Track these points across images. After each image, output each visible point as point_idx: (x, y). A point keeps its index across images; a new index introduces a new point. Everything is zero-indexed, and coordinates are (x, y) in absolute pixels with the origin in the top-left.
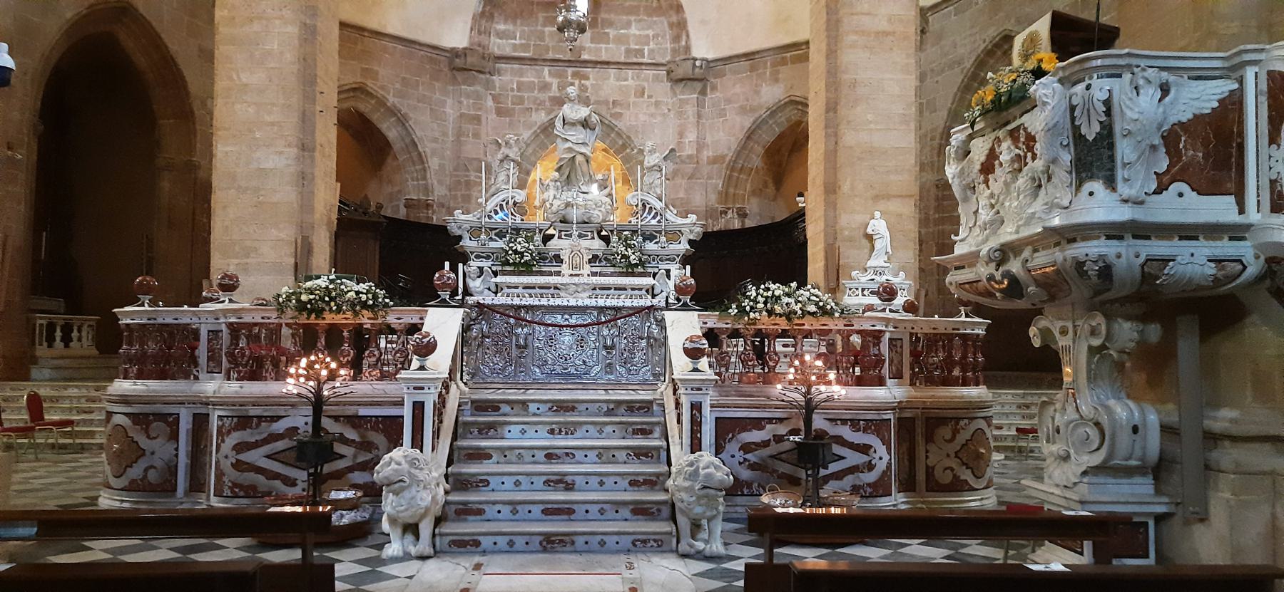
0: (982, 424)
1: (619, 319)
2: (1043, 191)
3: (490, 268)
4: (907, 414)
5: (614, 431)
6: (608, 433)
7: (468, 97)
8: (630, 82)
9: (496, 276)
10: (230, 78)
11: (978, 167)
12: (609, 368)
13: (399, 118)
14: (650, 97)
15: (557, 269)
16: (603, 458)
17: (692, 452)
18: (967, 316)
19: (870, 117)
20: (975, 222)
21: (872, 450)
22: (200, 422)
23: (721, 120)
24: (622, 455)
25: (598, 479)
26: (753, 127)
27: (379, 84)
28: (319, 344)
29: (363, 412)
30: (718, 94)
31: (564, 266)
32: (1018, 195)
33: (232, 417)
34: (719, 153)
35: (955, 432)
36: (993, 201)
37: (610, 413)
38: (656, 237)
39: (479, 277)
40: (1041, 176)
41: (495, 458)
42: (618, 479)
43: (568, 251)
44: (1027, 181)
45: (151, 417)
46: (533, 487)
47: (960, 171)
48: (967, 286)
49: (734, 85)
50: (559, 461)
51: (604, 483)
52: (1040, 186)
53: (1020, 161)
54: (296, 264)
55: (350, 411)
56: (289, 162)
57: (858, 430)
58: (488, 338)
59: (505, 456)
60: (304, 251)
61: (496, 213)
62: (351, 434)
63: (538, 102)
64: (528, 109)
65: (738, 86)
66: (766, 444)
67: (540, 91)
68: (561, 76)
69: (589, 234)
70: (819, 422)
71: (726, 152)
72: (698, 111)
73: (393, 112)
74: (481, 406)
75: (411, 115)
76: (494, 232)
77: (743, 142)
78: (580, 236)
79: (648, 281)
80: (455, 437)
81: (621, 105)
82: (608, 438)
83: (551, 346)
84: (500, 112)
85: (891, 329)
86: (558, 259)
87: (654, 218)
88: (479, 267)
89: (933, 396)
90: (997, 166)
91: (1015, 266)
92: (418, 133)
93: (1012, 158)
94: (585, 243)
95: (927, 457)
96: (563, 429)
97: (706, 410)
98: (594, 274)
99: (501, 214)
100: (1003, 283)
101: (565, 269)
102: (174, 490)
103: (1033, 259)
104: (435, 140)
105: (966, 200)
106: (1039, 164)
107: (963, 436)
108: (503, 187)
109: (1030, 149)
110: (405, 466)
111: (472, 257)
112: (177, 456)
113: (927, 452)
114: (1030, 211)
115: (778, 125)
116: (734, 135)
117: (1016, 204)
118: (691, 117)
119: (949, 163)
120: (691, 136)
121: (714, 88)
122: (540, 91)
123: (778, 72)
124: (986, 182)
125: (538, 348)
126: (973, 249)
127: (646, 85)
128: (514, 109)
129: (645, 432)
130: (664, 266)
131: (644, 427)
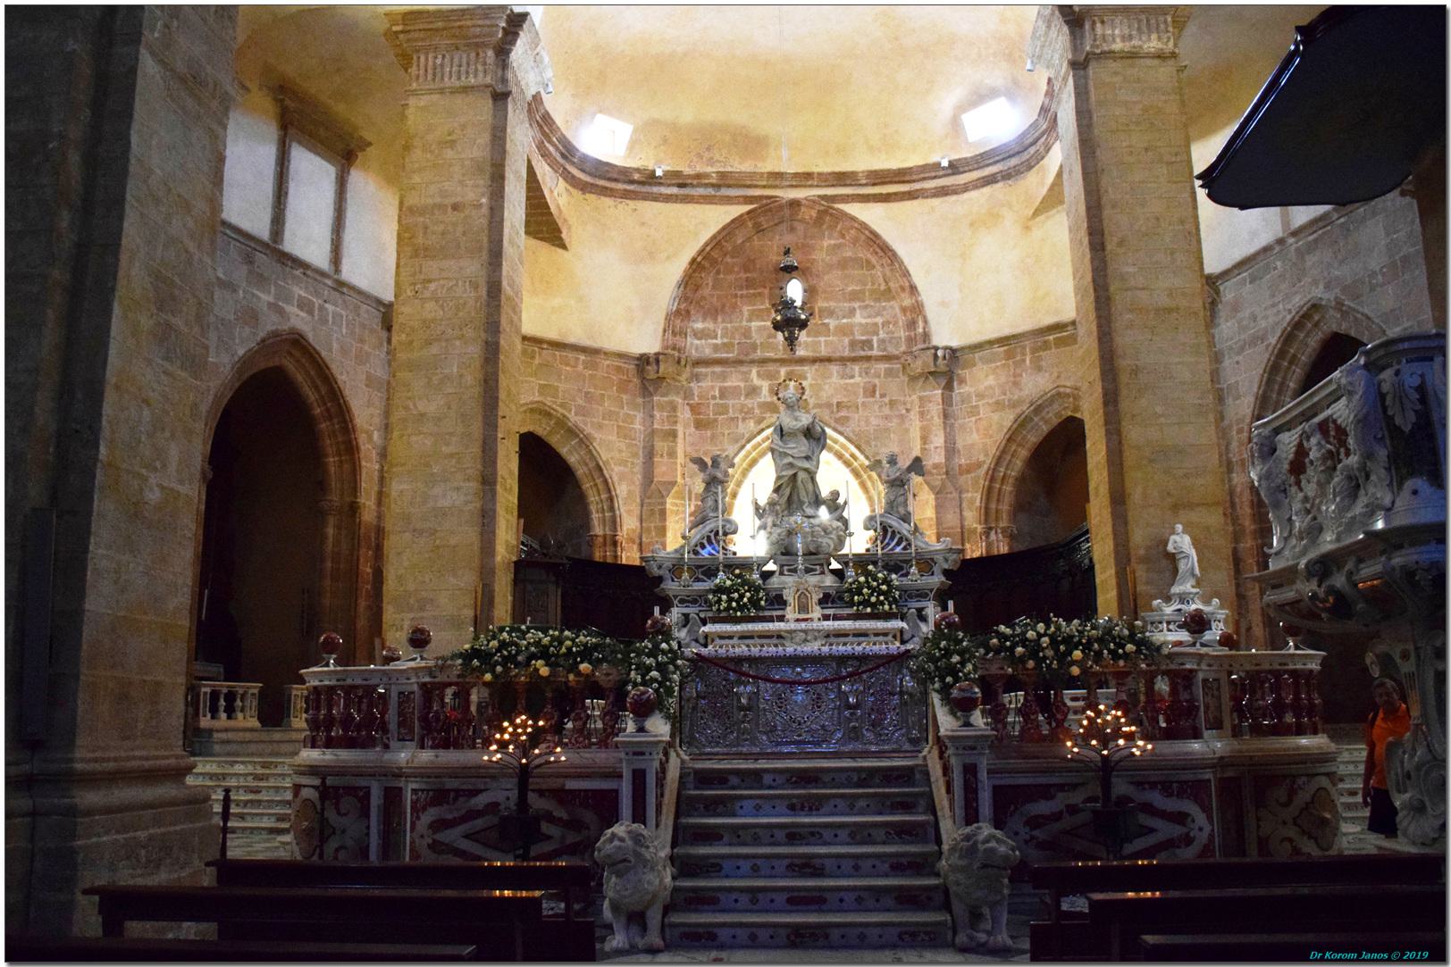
0: (1324, 782)
1: (863, 672)
2: (1362, 492)
3: (698, 615)
4: (1230, 773)
5: (868, 806)
7: (662, 408)
8: (857, 379)
9: (705, 624)
10: (406, 408)
11: (1286, 466)
13: (581, 439)
14: (883, 396)
15: (779, 613)
16: (858, 837)
17: (968, 823)
18: (1297, 648)
19: (1159, 409)
20: (1291, 531)
21: (1189, 819)
22: (393, 797)
23: (973, 419)
24: (880, 834)
25: (851, 862)
26: (1015, 426)
27: (559, 401)
28: (519, 706)
29: (571, 785)
30: (967, 389)
31: (789, 608)
32: (1335, 497)
33: (428, 791)
34: (974, 460)
35: (1292, 793)
36: (1308, 506)
37: (860, 784)
38: (902, 568)
39: (685, 626)
40: (1358, 474)
42: (877, 863)
44: (1343, 480)
45: (341, 791)
46: (774, 872)
47: (1267, 471)
48: (1287, 608)
49: (987, 376)
52: (1358, 486)
53: (1332, 458)
54: (476, 616)
56: (469, 498)
57: (1171, 795)
58: (704, 698)
60: (486, 600)
61: (703, 547)
62: (560, 813)
63: (746, 410)
64: (732, 419)
65: (991, 377)
66: (1057, 817)
67: (747, 396)
68: (770, 376)
69: (818, 567)
70: (1121, 787)
71: (982, 458)
72: (944, 410)
73: (572, 432)
74: (705, 778)
75: (596, 435)
77: (1003, 445)
78: (808, 571)
79: (898, 624)
80: (677, 816)
81: (848, 407)
83: (780, 707)
84: (699, 425)
85: (1204, 667)
86: (778, 601)
87: (898, 544)
88: (684, 614)
89: (1261, 750)
90: (1308, 465)
91: (1339, 581)
92: (604, 455)
93: (1323, 455)
94: (813, 580)
95: (1259, 827)
96: (806, 804)
97: (983, 775)
98: (826, 618)
100: (1327, 601)
101: (790, 613)
103: (1358, 571)
104: (623, 463)
105: (1277, 505)
106: (1353, 460)
107: (1303, 797)
108: (711, 514)
109: (1342, 443)
110: (629, 843)
111: (676, 602)
112: (368, 834)
113: (1259, 819)
114: (1349, 515)
115: (1046, 422)
116: (991, 437)
117: (1333, 507)
118: (936, 418)
119: (1253, 463)
120: (938, 440)
121: (962, 381)
122: (747, 396)
123: (1040, 358)
124: (1298, 483)
125: (764, 710)
126: (1291, 563)
127: (877, 381)
128: (716, 420)
129: (906, 805)
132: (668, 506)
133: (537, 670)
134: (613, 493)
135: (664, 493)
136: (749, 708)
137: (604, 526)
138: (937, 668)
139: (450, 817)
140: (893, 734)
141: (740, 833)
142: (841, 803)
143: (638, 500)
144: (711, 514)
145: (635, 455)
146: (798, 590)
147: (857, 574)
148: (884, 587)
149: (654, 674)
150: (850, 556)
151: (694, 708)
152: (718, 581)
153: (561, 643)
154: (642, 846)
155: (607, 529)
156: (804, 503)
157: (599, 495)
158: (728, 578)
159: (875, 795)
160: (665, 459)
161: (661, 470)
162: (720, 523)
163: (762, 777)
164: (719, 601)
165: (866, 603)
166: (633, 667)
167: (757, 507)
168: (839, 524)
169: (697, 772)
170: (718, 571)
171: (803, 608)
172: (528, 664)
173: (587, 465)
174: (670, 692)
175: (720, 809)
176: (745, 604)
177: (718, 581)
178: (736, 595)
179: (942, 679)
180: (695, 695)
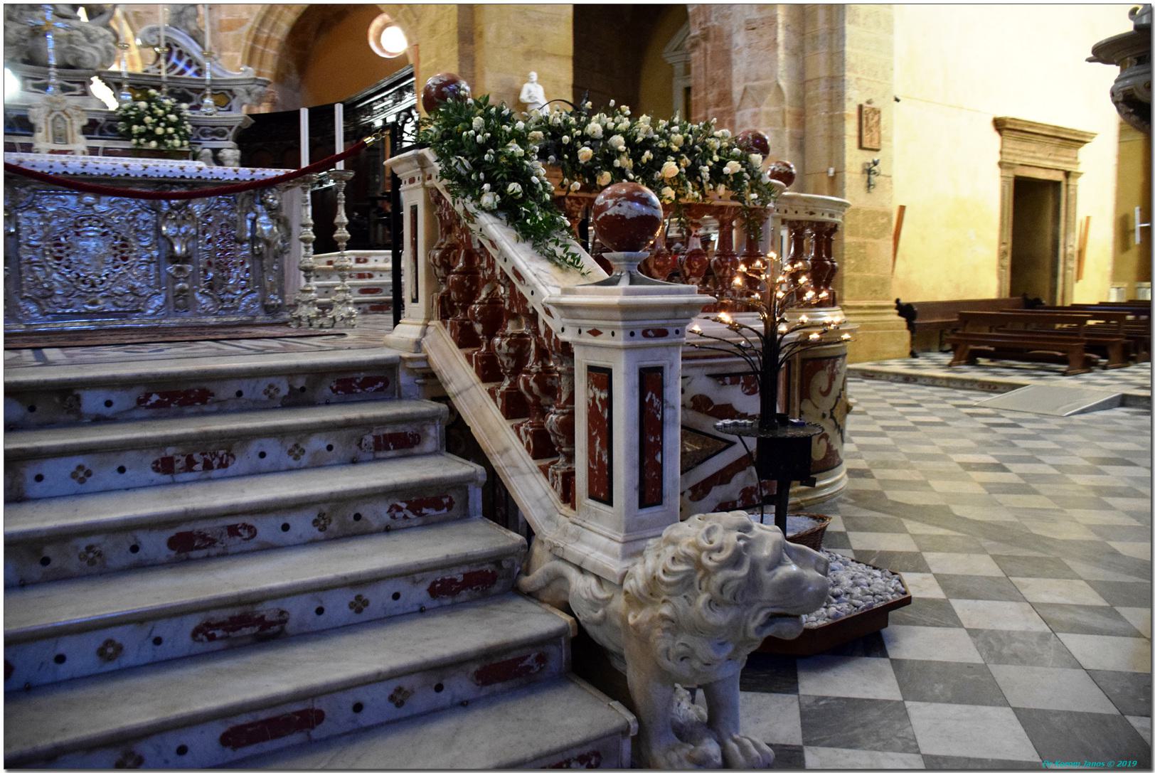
5: (330, 448)
6: (315, 454)
12: (181, 301)
16: (334, 526)
24: (378, 513)
25: (349, 596)
37: (296, 400)
42: (402, 586)
46: (163, 651)
50: (213, 551)
51: (366, 603)
82: (317, 465)
96: (196, 457)
97: (675, 394)
98: (93, 151)
130: (207, 146)
131: (400, 428)
138: (477, 166)
140: (240, 300)
142: (274, 449)
147: (135, 100)
148: (173, 117)
159: (348, 424)
163: (78, 398)
165: (150, 135)
179: (498, 188)
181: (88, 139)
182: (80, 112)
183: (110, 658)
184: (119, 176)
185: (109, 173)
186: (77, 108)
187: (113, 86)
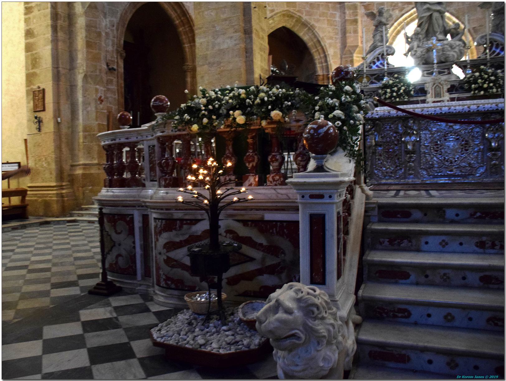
3: (373, 102)
15: (422, 98)
28: (227, 152)
29: (269, 216)
33: (162, 219)
41: (413, 278)
43: (431, 84)
45: (116, 217)
55: (256, 215)
58: (380, 146)
59: (427, 276)
62: (261, 240)
69: (446, 70)
76: (374, 77)
78: (440, 73)
83: (437, 151)
92: (321, 35)
98: (452, 99)
99: (378, 63)
101: (430, 98)
102: (135, 274)
104: (331, 38)
110: (298, 314)
112: (134, 247)
125: (425, 153)
132: (355, 58)
133: (234, 119)
134: (327, 53)
135: (352, 51)
136: (413, 152)
137: (323, 70)
139: (178, 240)
141: (428, 272)
143: (339, 56)
144: (379, 44)
145: (337, 34)
146: (434, 84)
147: (473, 72)
149: (338, 112)
150: (469, 62)
151: (374, 153)
152: (384, 82)
153: (256, 96)
154: (315, 318)
155: (324, 71)
156: (437, 32)
157: (319, 54)
158: (390, 79)
160: (352, 34)
161: (350, 41)
162: (385, 49)
163: (444, 212)
164: (385, 93)
166: (317, 108)
167: (407, 38)
168: (461, 43)
169: (381, 206)
170: (384, 76)
171: (438, 95)
172: (228, 115)
173: (312, 40)
174: (354, 130)
175: (405, 243)
176: (401, 93)
177: (384, 82)
178: (396, 89)
180: (374, 144)
181: (450, 94)
182: (446, 82)
183: (449, 321)
184: (465, 112)
185: (461, 111)
186: (445, 81)
187: (463, 67)
